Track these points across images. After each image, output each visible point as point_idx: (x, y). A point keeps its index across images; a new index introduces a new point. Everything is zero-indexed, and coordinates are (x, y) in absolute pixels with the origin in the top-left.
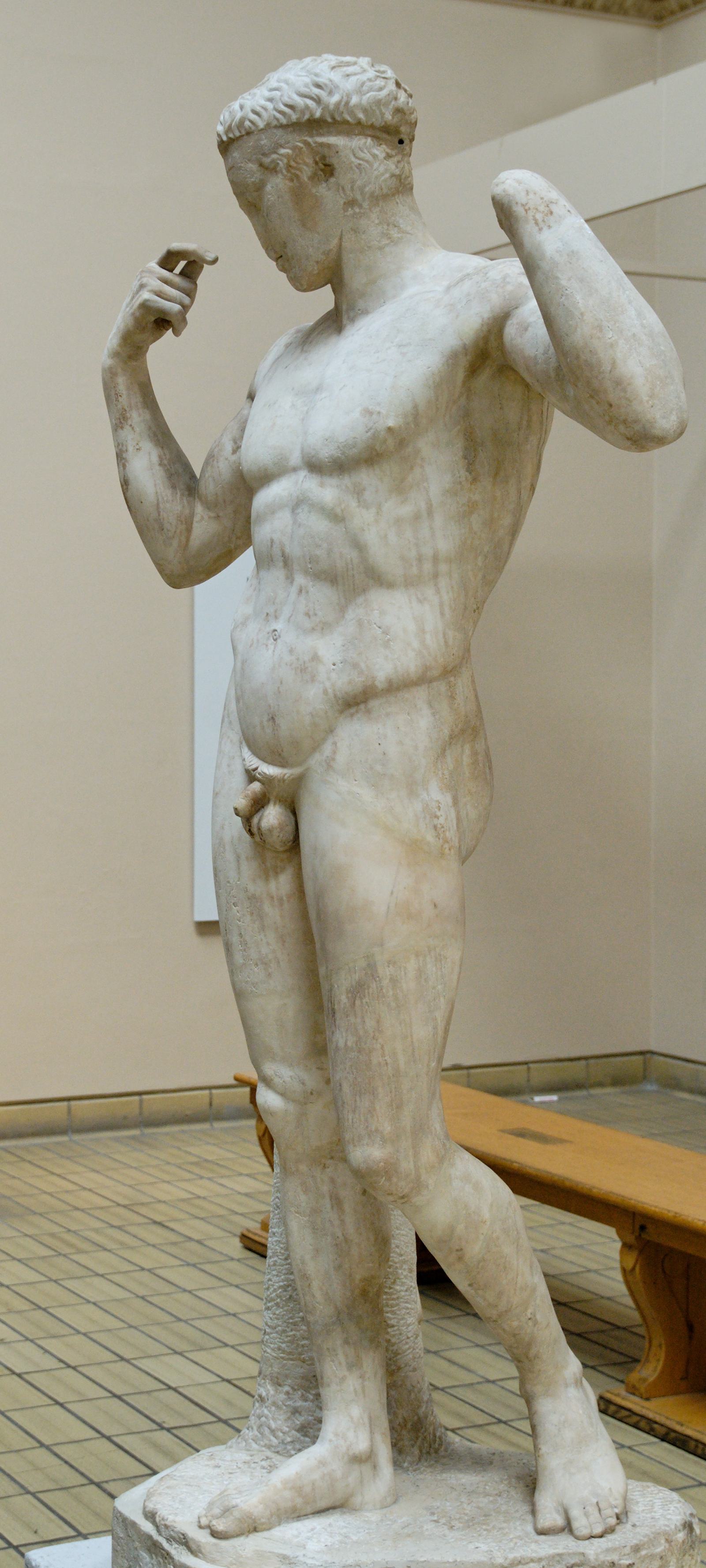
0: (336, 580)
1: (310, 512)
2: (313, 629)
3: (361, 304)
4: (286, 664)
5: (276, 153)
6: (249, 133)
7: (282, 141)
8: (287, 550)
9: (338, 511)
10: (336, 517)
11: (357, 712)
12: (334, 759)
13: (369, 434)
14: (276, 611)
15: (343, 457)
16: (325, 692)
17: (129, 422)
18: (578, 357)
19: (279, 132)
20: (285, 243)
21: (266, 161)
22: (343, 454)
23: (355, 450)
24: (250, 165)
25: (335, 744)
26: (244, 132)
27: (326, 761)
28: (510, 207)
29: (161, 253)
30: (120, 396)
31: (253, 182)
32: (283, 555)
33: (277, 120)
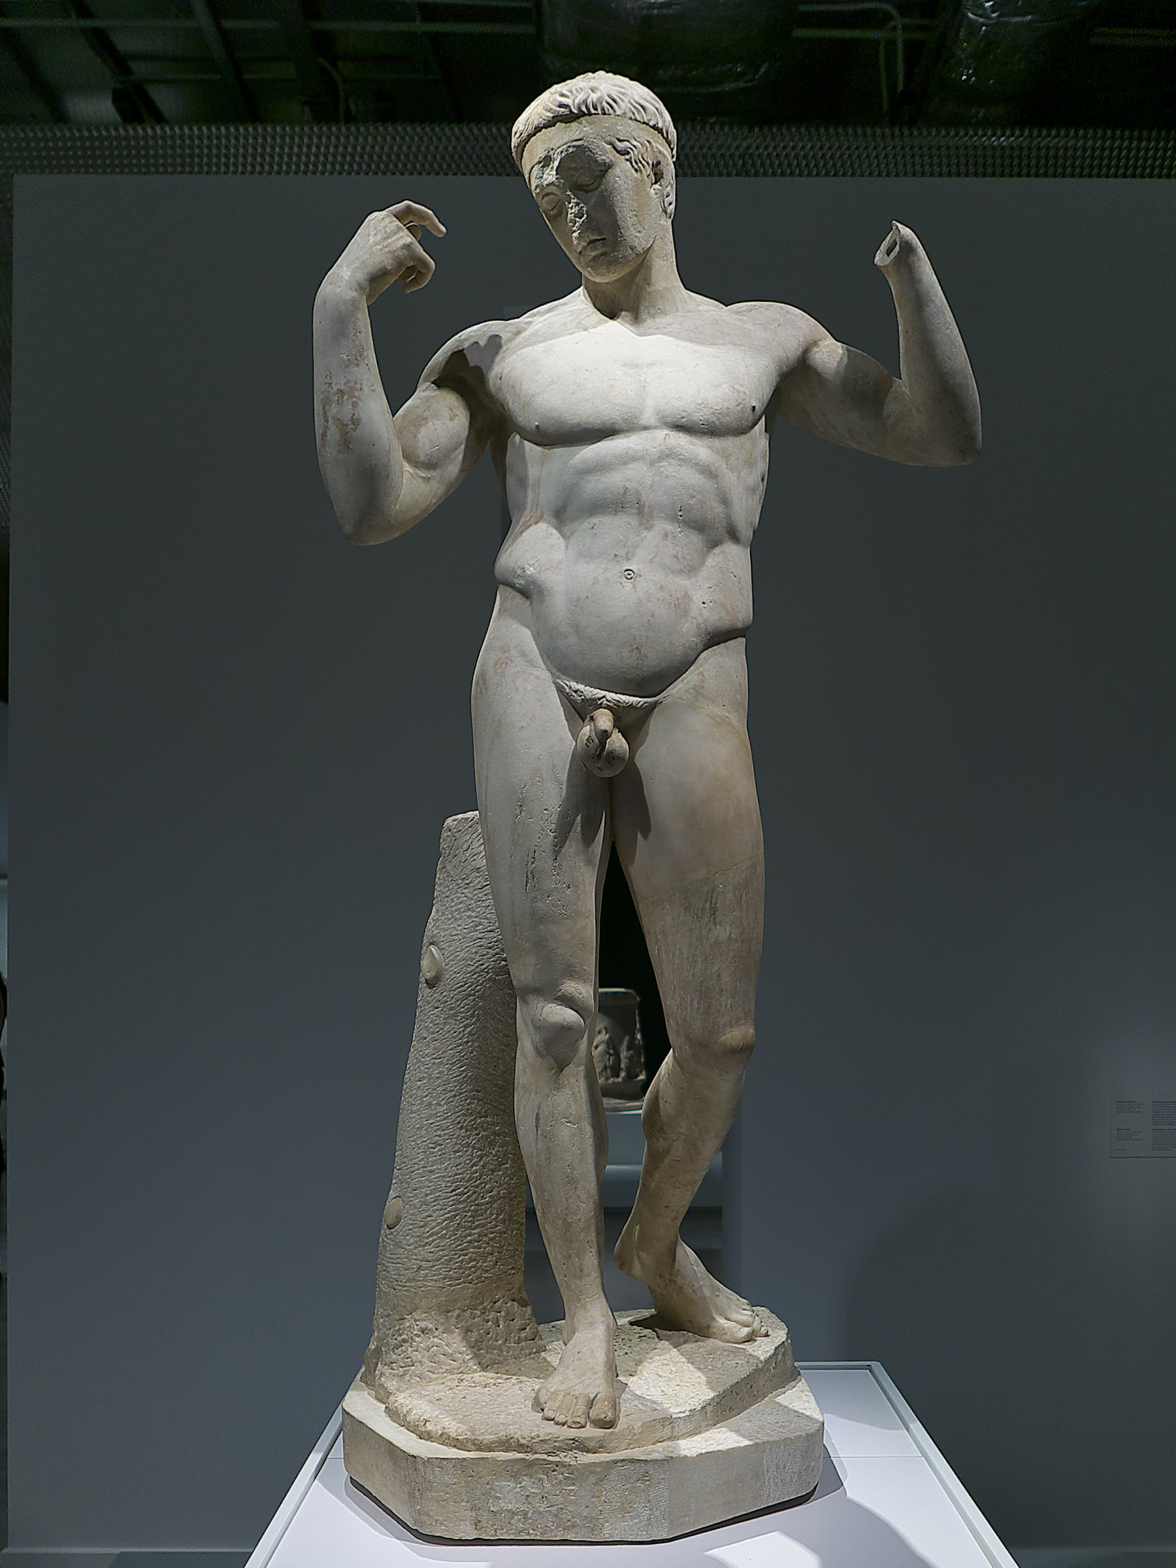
3: (660, 304)
4: (658, 600)
14: (627, 553)
30: (360, 332)
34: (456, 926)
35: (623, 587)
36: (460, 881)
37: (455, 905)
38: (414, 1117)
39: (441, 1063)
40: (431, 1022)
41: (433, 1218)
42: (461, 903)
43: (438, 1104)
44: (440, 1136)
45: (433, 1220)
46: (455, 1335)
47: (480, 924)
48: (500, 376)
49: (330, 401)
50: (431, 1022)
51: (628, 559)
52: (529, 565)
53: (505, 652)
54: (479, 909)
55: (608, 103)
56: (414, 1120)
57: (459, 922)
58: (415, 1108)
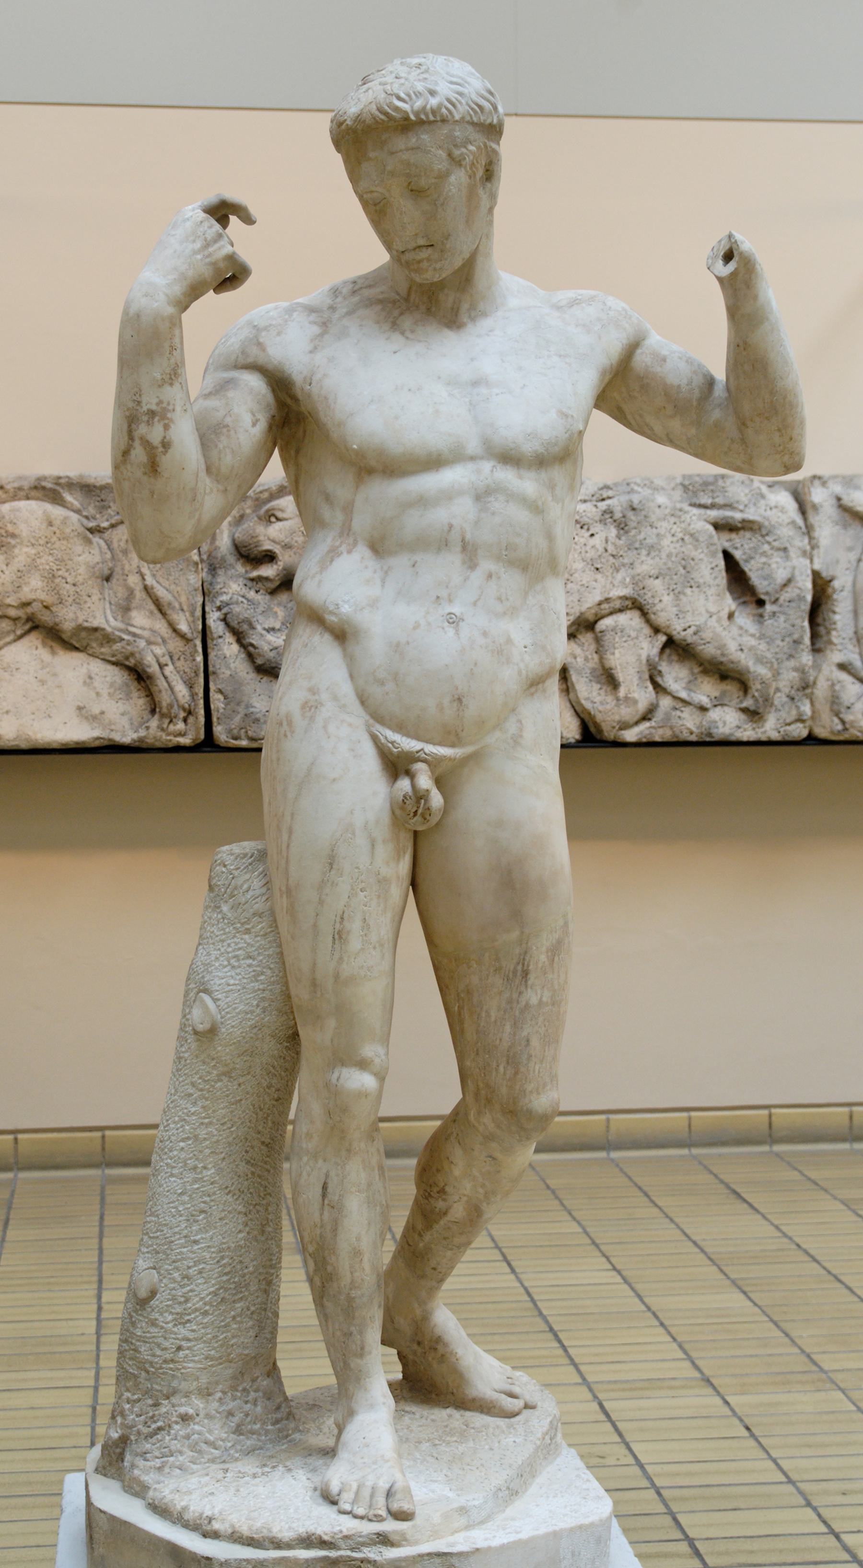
0: (527, 568)
1: (507, 501)
2: (505, 613)
4: (481, 646)
5: (465, 147)
6: (444, 121)
7: (472, 138)
8: (468, 536)
9: (540, 503)
10: (536, 508)
11: (536, 691)
12: (521, 736)
13: (567, 435)
14: (449, 595)
15: (546, 453)
16: (520, 673)
17: (180, 380)
18: (785, 398)
19: (470, 128)
20: (449, 235)
21: (457, 152)
22: (547, 450)
23: (557, 449)
24: (440, 152)
25: (520, 721)
26: (438, 119)
27: (512, 738)
28: (755, 265)
29: (211, 197)
31: (439, 170)
32: (463, 540)
33: (471, 116)
34: (233, 974)
35: (445, 633)
36: (239, 925)
37: (234, 951)
38: (175, 1182)
39: (211, 1123)
40: (200, 1078)
41: (196, 1293)
42: (240, 949)
43: (205, 1168)
44: (204, 1202)
45: (196, 1295)
46: (216, 1420)
47: (262, 973)
50: (200, 1078)
51: (450, 601)
52: (343, 601)
53: (314, 694)
54: (261, 958)
55: (447, 109)
56: (175, 1184)
57: (238, 971)
58: (175, 1171)
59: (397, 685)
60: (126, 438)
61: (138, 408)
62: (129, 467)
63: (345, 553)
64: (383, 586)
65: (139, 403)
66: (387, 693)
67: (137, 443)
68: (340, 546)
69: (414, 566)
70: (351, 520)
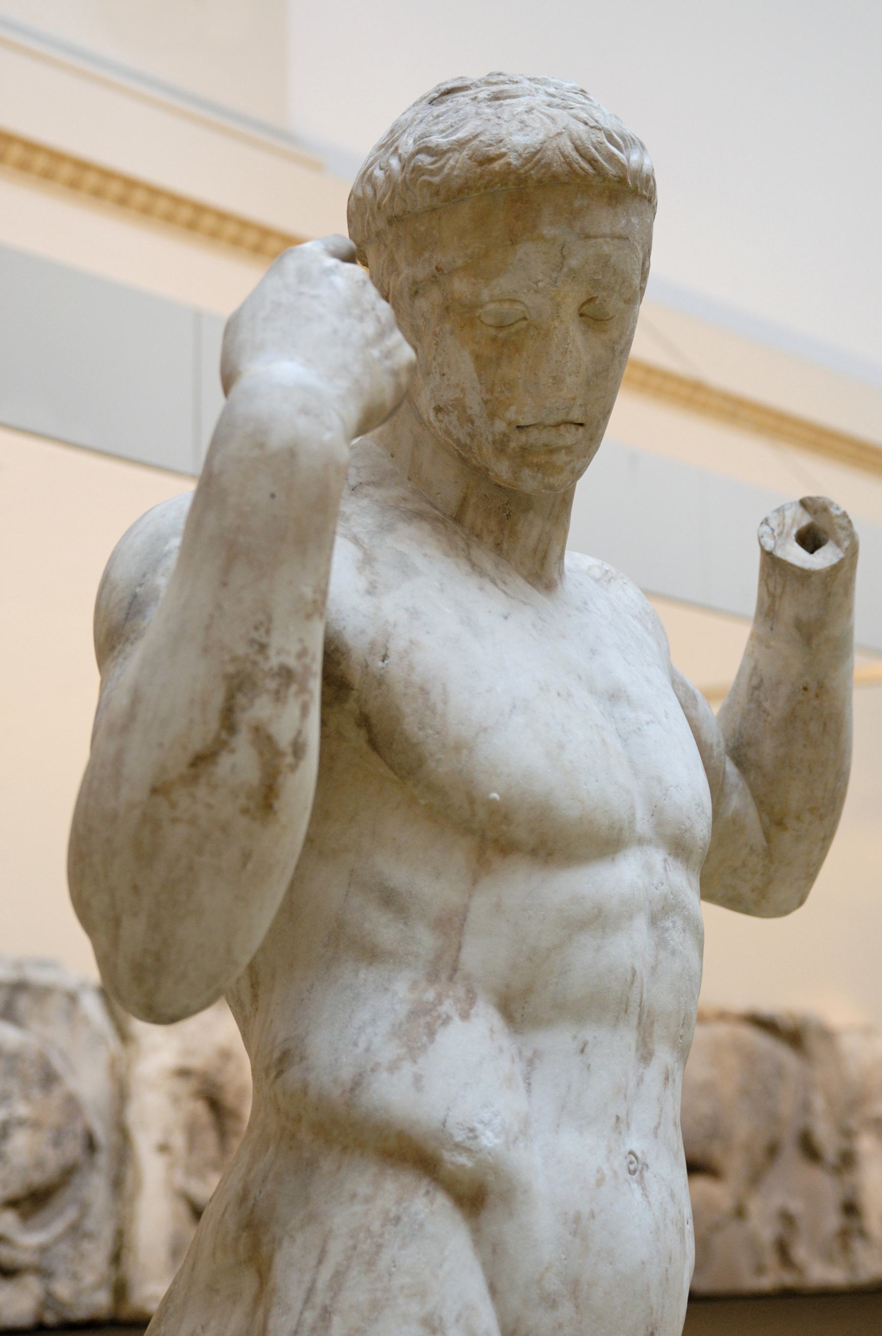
48: (383, 653)
49: (254, 685)
52: (482, 1122)
59: (577, 1307)
60: (214, 724)
61: (259, 658)
62: (201, 792)
63: (457, 1020)
64: (529, 1091)
65: (263, 648)
66: (560, 1326)
67: (243, 741)
68: (439, 1000)
69: (582, 1051)
70: (459, 949)
